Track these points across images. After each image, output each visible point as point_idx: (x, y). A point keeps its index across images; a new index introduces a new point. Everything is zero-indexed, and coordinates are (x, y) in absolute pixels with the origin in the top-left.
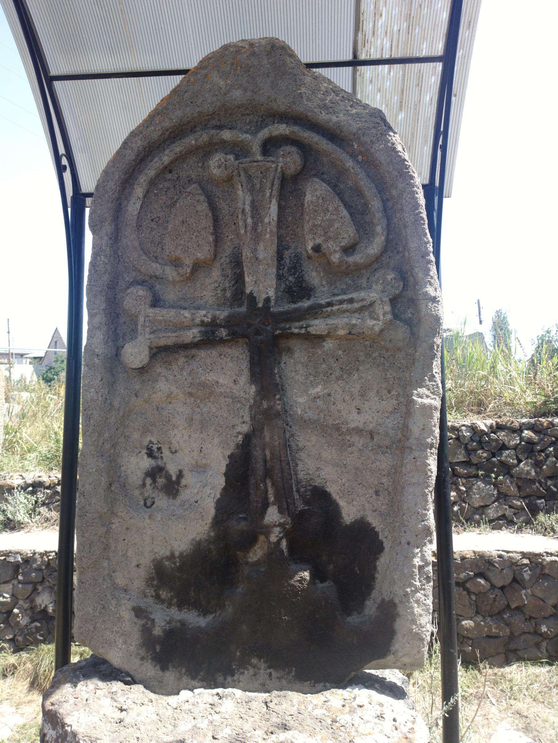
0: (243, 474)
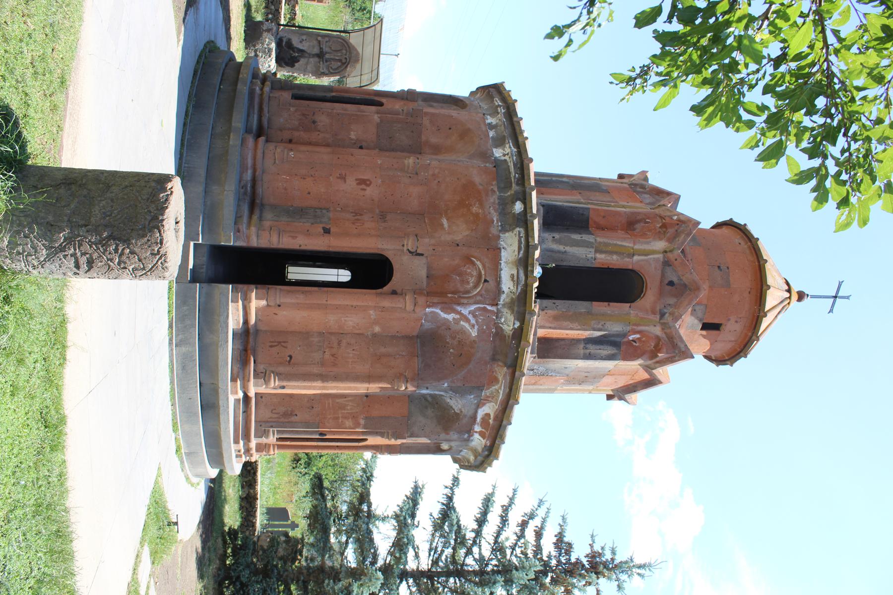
0: (302, 51)
